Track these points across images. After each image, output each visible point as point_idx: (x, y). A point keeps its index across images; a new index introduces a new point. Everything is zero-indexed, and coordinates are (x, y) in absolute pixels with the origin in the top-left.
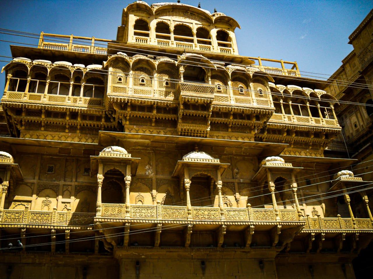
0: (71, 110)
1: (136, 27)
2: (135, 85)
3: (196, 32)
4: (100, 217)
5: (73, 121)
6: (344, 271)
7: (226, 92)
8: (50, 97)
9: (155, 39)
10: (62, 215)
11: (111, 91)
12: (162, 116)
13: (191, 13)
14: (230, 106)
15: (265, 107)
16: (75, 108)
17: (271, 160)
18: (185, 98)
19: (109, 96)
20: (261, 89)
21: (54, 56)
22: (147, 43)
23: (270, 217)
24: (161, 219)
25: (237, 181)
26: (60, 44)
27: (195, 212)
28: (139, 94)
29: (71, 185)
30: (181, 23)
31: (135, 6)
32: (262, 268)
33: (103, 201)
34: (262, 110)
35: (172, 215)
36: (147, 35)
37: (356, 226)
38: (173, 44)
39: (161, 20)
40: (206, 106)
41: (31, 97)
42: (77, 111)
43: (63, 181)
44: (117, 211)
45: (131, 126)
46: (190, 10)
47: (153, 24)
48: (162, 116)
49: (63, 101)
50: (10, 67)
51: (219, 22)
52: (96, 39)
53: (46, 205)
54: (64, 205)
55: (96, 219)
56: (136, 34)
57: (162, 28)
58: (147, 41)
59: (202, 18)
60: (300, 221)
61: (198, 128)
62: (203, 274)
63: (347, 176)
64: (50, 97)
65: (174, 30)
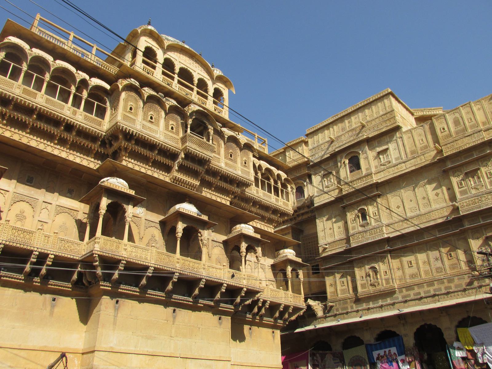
0: (69, 122)
2: (144, 119)
6: (274, 337)
10: (47, 238)
11: (122, 118)
12: (160, 158)
14: (221, 168)
16: (75, 121)
18: (189, 149)
19: (119, 123)
24: (153, 263)
26: (58, 38)
27: (182, 261)
28: (146, 130)
29: (51, 204)
30: (186, 67)
33: (103, 233)
34: (244, 179)
35: (163, 261)
38: (175, 86)
41: (25, 91)
43: (43, 198)
44: (115, 246)
45: (130, 160)
46: (196, 57)
48: (160, 158)
50: (5, 45)
53: (20, 220)
55: (95, 250)
57: (168, 65)
60: (260, 288)
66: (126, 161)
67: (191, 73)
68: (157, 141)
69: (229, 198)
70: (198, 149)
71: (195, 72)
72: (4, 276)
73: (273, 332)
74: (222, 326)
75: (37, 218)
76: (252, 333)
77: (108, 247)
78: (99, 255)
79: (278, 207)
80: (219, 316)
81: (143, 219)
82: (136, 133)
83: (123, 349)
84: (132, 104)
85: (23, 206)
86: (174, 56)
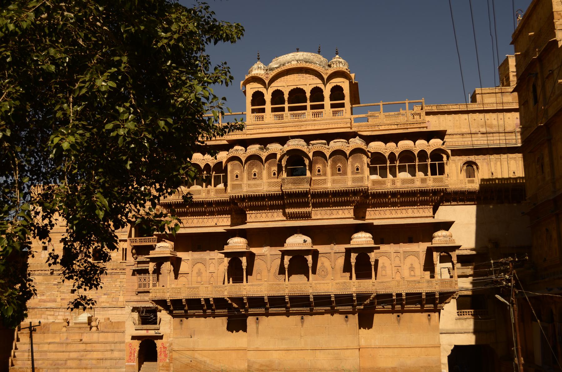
1: (253, 104)
2: (249, 179)
6: (429, 320)
9: (270, 115)
13: (305, 71)
15: (360, 184)
16: (209, 199)
17: (357, 238)
20: (359, 165)
22: (263, 120)
23: (348, 287)
25: (334, 251)
28: (252, 188)
30: (295, 87)
32: (347, 321)
36: (263, 110)
37: (437, 286)
39: (276, 88)
40: (305, 194)
42: (210, 201)
45: (251, 212)
49: (200, 194)
54: (211, 274)
56: (253, 111)
57: (277, 96)
58: (263, 118)
59: (317, 75)
62: (302, 326)
63: (441, 238)
66: (249, 214)
67: (302, 89)
68: (262, 193)
70: (293, 187)
71: (306, 85)
72: (195, 313)
73: (429, 315)
74: (348, 323)
75: (208, 271)
76: (400, 319)
79: (423, 189)
80: (345, 315)
81: (268, 255)
82: (244, 195)
83: (265, 348)
84: (237, 172)
85: (199, 266)
86: (279, 85)
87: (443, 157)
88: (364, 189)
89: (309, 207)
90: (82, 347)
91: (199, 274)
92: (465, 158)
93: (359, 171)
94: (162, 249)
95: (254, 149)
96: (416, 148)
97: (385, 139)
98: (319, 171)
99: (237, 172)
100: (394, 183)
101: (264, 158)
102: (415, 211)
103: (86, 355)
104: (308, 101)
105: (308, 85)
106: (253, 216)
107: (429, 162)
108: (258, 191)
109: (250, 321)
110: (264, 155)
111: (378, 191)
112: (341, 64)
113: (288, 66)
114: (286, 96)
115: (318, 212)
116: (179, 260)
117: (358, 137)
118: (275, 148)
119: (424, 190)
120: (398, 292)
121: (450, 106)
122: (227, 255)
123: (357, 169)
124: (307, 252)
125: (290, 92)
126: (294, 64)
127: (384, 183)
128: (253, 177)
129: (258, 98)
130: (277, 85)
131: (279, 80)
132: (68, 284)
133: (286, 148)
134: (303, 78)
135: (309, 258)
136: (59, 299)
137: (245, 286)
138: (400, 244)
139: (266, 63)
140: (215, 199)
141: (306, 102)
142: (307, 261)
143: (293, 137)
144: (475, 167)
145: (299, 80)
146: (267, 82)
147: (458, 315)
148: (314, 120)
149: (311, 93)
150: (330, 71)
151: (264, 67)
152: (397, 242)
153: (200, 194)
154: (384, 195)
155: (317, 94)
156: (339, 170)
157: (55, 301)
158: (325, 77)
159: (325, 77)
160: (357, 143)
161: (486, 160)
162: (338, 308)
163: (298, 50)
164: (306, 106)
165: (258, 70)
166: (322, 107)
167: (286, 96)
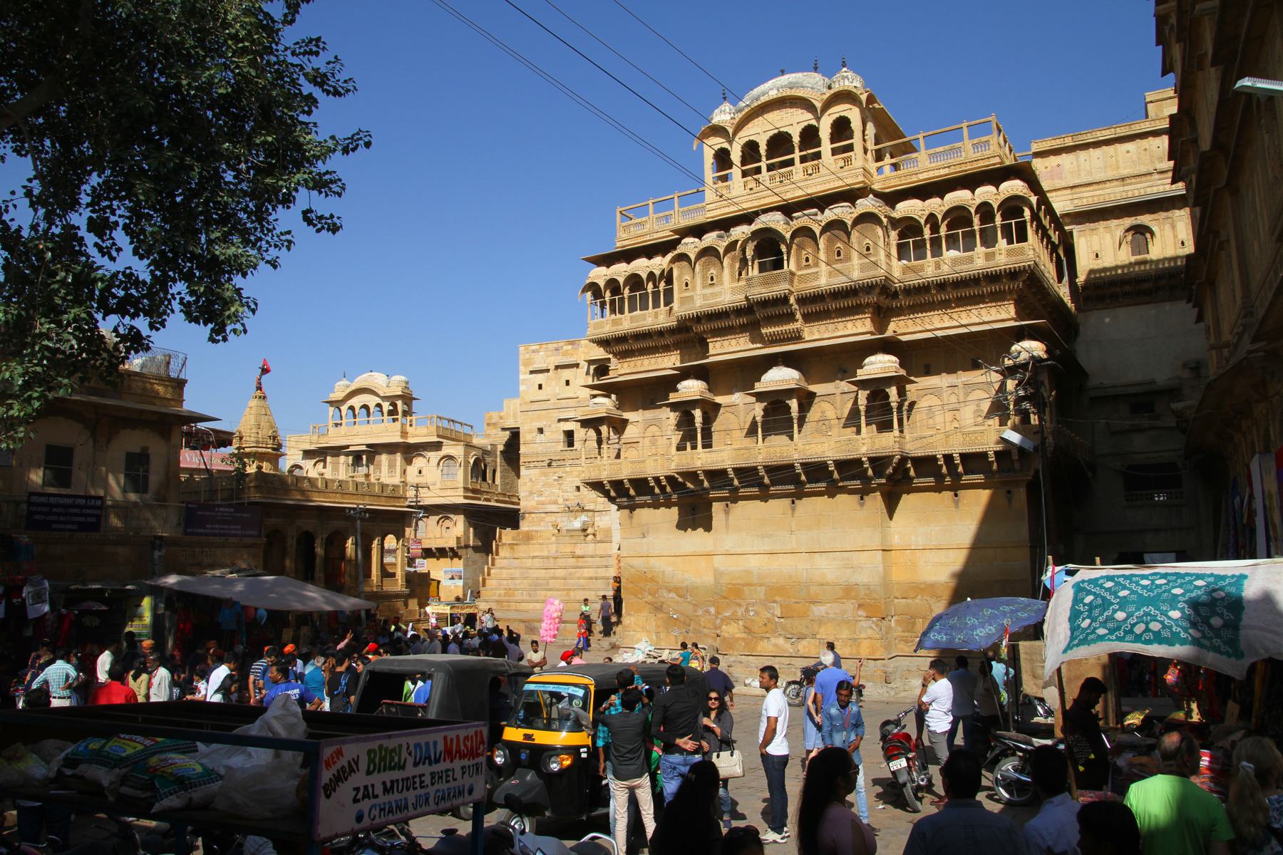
2: (703, 287)
3: (799, 139)
4: (673, 467)
5: (663, 342)
6: (1010, 501)
7: (816, 265)
8: (631, 317)
13: (791, 103)
20: (870, 242)
21: (628, 255)
25: (839, 391)
30: (776, 131)
31: (707, 132)
32: (862, 505)
39: (747, 139)
40: (784, 300)
41: (615, 323)
45: (715, 339)
47: (736, 156)
51: (834, 102)
52: (679, 194)
57: (751, 150)
61: (781, 328)
64: (631, 317)
65: (767, 151)
67: (787, 133)
69: (865, 313)
70: (763, 291)
73: (1009, 492)
74: (865, 507)
77: (684, 461)
78: (677, 473)
81: (741, 405)
87: (1023, 211)
88: (879, 281)
89: (797, 321)
90: (572, 561)
91: (653, 443)
92: (1129, 222)
93: (871, 251)
94: (596, 407)
95: (710, 239)
96: (974, 202)
97: (923, 192)
98: (807, 260)
99: (688, 277)
100: (938, 266)
101: (721, 251)
102: (984, 312)
103: (575, 573)
104: (797, 150)
105: (795, 125)
106: (718, 345)
107: (998, 220)
108: (716, 304)
109: (717, 507)
110: (721, 246)
111: (911, 283)
112: (846, 80)
113: (763, 99)
114: (763, 149)
115: (815, 329)
116: (625, 422)
117: (871, 196)
118: (741, 232)
119: (992, 272)
120: (946, 452)
121: (1098, 133)
122: (674, 407)
123: (868, 249)
124: (789, 393)
125: (768, 141)
126: (773, 94)
127: (922, 268)
128: (710, 282)
129: (722, 159)
130: (749, 133)
131: (750, 125)
132: (571, 479)
133: (754, 227)
134: (788, 115)
135: (794, 404)
136: (561, 501)
137: (698, 454)
138: (959, 372)
139: (734, 105)
140: (664, 325)
141: (794, 153)
142: (790, 408)
143: (765, 211)
144: (1148, 235)
145: (782, 119)
146: (731, 131)
147: (1127, 500)
148: (806, 180)
149: (800, 137)
150: (829, 93)
151: (730, 109)
152: (951, 371)
153: (645, 319)
154: (923, 289)
155: (810, 136)
156: (839, 254)
157: (556, 503)
158: (818, 105)
159: (818, 105)
160: (867, 204)
161: (1170, 220)
162: (846, 483)
163: (783, 72)
164: (793, 159)
165: (723, 115)
166: (817, 156)
167: (763, 149)
